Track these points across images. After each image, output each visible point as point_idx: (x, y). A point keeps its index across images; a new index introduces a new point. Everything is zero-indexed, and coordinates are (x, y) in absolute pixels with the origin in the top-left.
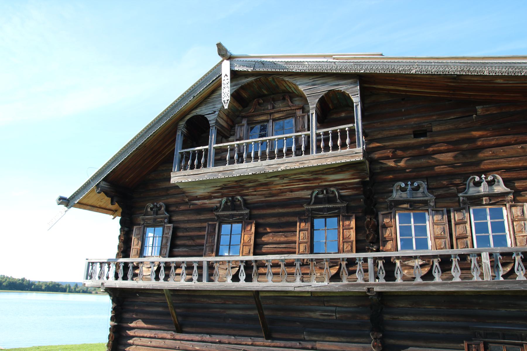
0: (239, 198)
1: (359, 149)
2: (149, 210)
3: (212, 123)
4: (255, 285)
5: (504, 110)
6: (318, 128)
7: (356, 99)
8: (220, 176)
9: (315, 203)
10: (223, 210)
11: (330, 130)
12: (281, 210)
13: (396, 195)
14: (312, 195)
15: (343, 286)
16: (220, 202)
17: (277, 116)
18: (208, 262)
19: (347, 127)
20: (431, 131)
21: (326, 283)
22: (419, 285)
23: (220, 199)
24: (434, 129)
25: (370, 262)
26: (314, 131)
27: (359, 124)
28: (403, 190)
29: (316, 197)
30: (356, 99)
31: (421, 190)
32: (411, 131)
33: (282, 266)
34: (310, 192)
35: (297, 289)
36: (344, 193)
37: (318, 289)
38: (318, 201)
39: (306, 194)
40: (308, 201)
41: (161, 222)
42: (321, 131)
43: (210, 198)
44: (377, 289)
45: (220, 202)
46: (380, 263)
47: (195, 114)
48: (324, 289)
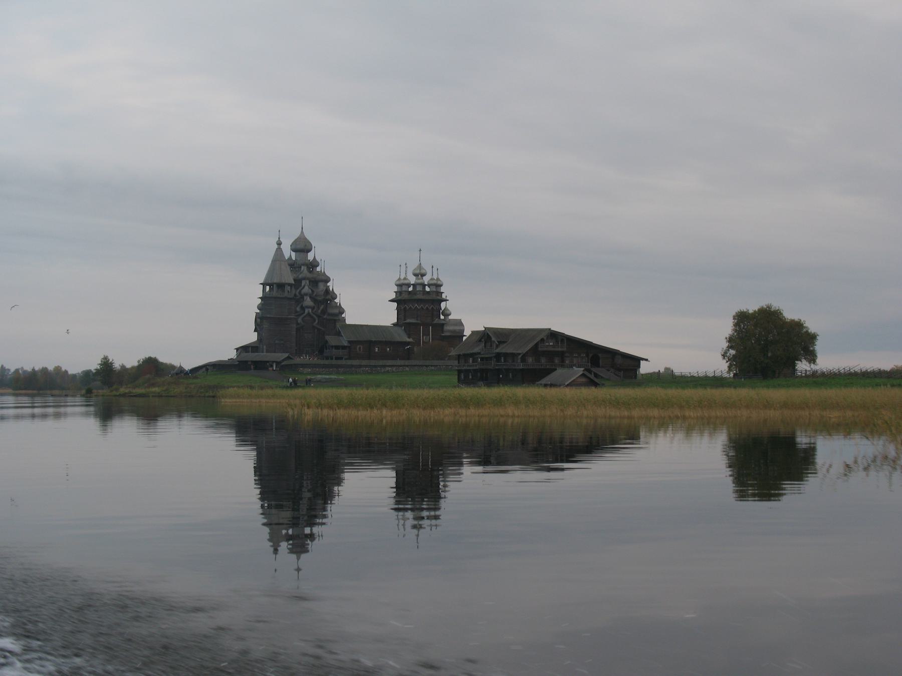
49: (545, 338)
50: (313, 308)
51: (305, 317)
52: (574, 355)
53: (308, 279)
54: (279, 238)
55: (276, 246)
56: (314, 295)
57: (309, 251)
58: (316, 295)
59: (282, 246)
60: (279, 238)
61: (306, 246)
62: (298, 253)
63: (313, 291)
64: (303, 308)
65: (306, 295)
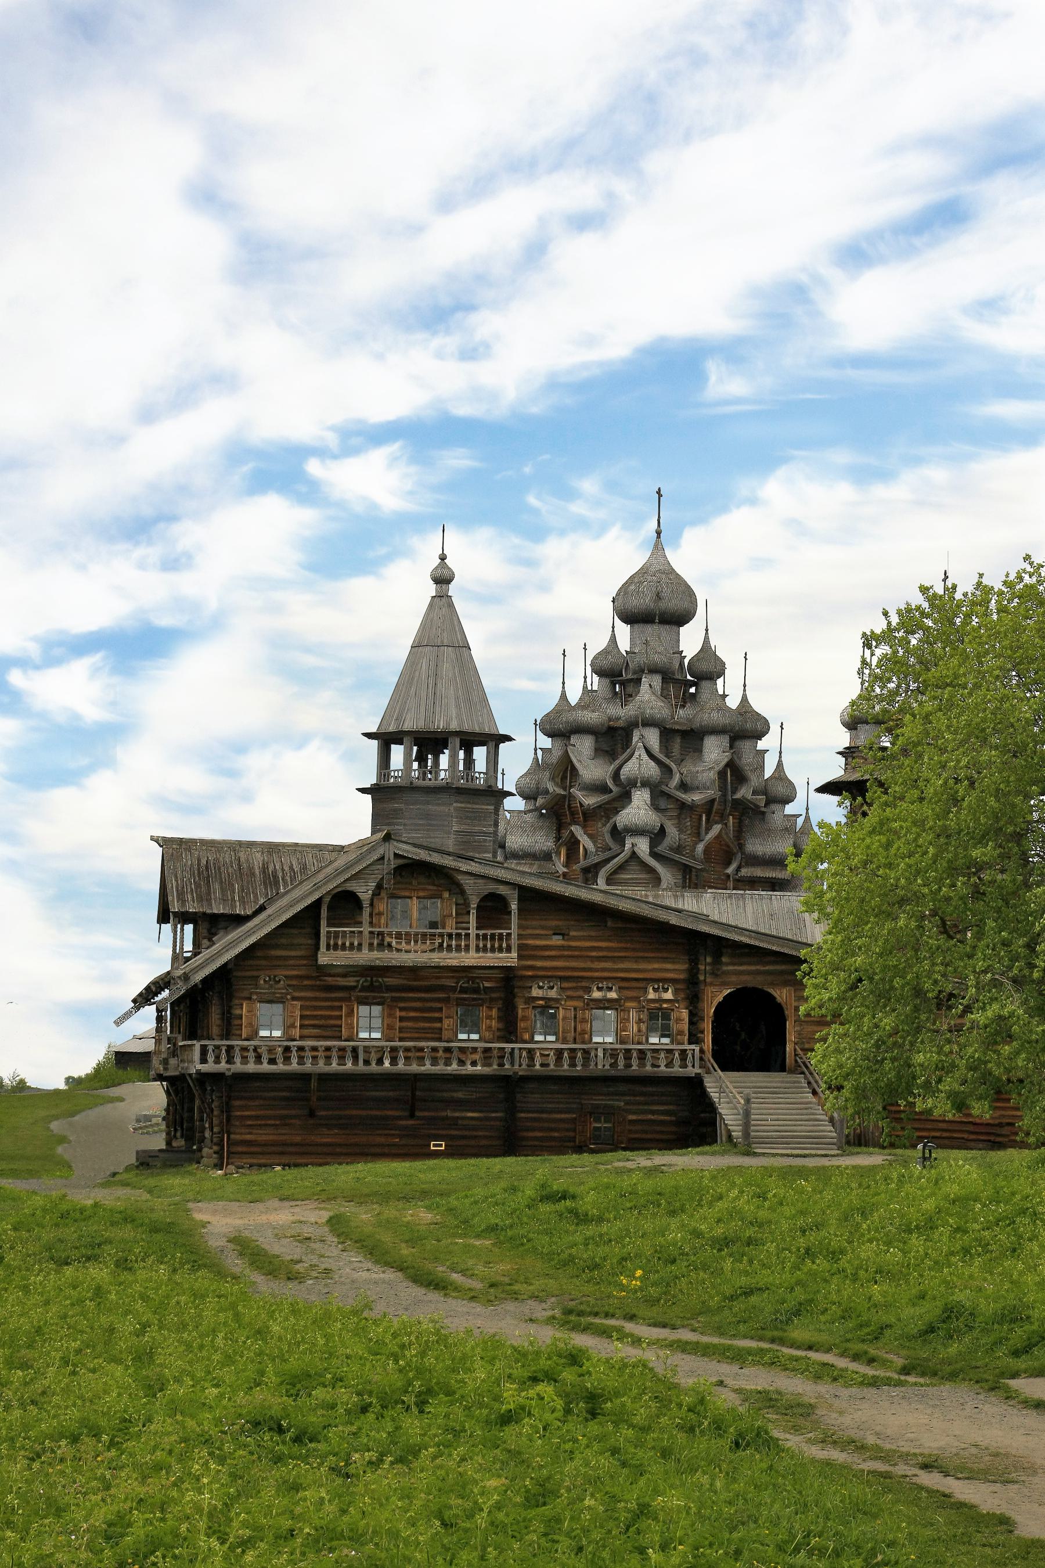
0: (380, 980)
1: (514, 954)
2: (262, 982)
3: (366, 904)
4: (414, 1068)
5: (628, 926)
6: (478, 928)
7: (514, 906)
8: (378, 963)
9: (461, 992)
10: (360, 991)
11: (489, 932)
12: (423, 995)
13: (536, 992)
14: (457, 983)
15: (494, 1070)
16: (358, 981)
17: (421, 894)
18: (365, 1047)
19: (504, 932)
20: (568, 935)
21: (479, 1068)
22: (552, 1070)
23: (358, 978)
24: (572, 933)
25: (517, 1052)
26: (473, 931)
27: (514, 929)
28: (540, 988)
29: (461, 986)
30: (514, 906)
31: (555, 989)
32: (551, 932)
33: (441, 1052)
34: (455, 981)
35: (454, 1072)
36: (487, 984)
37: (474, 1073)
38: (463, 990)
39: (451, 983)
40: (453, 989)
41: (282, 998)
42: (481, 932)
43: (345, 976)
44: (520, 1073)
45: (358, 981)
46: (524, 1053)
47: (344, 889)
48: (478, 1072)
49: (364, 891)
50: (657, 836)
51: (621, 868)
52: (597, 994)
53: (648, 723)
54: (443, 558)
55: (432, 589)
56: (676, 780)
57: (682, 618)
58: (684, 786)
59: (453, 589)
60: (443, 558)
61: (658, 596)
62: (636, 626)
63: (666, 770)
64: (618, 835)
65: (633, 783)
